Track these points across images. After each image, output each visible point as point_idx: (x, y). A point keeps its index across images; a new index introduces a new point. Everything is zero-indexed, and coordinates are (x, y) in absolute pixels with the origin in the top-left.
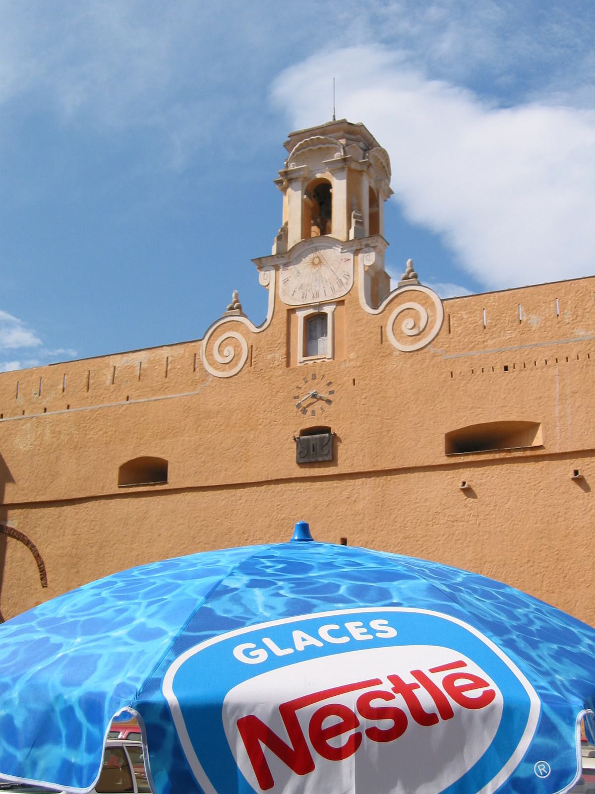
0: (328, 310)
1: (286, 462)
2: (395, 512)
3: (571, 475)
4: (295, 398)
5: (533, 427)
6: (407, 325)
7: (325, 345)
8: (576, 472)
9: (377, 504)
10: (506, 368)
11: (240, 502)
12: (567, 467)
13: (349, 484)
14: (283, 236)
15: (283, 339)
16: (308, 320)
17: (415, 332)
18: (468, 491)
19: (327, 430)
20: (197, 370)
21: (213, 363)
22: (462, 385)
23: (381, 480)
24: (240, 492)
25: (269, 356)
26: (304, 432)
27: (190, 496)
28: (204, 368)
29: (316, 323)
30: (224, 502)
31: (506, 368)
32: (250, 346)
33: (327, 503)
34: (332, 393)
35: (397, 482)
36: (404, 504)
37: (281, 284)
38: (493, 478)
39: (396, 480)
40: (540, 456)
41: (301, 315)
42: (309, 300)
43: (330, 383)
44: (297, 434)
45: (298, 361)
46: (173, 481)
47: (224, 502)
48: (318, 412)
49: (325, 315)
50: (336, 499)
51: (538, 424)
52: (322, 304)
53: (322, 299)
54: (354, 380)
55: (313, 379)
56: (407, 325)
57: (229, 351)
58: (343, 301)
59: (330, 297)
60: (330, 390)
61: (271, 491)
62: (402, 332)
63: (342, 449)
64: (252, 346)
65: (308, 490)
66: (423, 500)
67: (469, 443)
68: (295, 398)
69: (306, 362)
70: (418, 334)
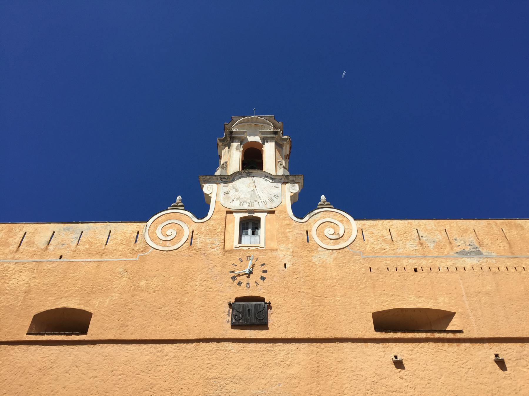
2: (331, 379)
3: (493, 357)
4: (231, 272)
5: (449, 316)
8: (497, 356)
9: (312, 369)
10: (416, 270)
11: (167, 358)
13: (283, 348)
15: (220, 229)
18: (399, 364)
19: (262, 300)
22: (381, 277)
23: (314, 346)
24: (168, 347)
26: (237, 300)
27: (110, 348)
29: (250, 224)
30: (148, 357)
31: (416, 270)
32: (191, 231)
33: (261, 365)
34: (265, 271)
35: (330, 350)
36: (340, 371)
38: (422, 355)
39: (329, 349)
41: (238, 216)
42: (246, 206)
43: (264, 264)
44: (232, 301)
45: (234, 246)
46: (92, 333)
47: (148, 357)
50: (270, 362)
51: (454, 313)
52: (254, 212)
53: (256, 207)
54: (285, 265)
55: (247, 260)
58: (273, 212)
59: (262, 207)
60: (264, 269)
61: (202, 349)
63: (273, 318)
64: (193, 231)
65: (240, 352)
66: (358, 369)
67: (393, 323)
68: (231, 272)
69: (240, 248)
70: (339, 239)
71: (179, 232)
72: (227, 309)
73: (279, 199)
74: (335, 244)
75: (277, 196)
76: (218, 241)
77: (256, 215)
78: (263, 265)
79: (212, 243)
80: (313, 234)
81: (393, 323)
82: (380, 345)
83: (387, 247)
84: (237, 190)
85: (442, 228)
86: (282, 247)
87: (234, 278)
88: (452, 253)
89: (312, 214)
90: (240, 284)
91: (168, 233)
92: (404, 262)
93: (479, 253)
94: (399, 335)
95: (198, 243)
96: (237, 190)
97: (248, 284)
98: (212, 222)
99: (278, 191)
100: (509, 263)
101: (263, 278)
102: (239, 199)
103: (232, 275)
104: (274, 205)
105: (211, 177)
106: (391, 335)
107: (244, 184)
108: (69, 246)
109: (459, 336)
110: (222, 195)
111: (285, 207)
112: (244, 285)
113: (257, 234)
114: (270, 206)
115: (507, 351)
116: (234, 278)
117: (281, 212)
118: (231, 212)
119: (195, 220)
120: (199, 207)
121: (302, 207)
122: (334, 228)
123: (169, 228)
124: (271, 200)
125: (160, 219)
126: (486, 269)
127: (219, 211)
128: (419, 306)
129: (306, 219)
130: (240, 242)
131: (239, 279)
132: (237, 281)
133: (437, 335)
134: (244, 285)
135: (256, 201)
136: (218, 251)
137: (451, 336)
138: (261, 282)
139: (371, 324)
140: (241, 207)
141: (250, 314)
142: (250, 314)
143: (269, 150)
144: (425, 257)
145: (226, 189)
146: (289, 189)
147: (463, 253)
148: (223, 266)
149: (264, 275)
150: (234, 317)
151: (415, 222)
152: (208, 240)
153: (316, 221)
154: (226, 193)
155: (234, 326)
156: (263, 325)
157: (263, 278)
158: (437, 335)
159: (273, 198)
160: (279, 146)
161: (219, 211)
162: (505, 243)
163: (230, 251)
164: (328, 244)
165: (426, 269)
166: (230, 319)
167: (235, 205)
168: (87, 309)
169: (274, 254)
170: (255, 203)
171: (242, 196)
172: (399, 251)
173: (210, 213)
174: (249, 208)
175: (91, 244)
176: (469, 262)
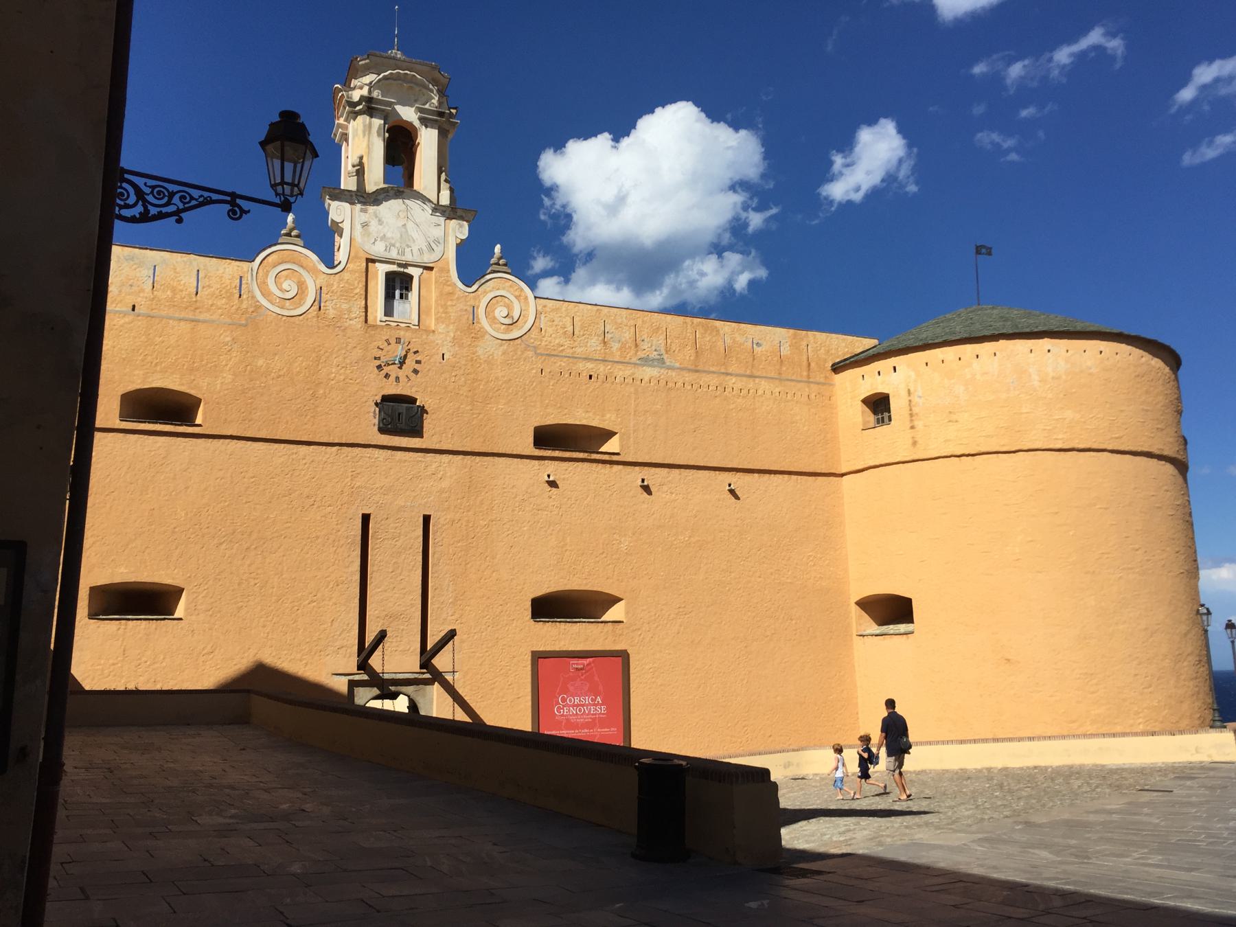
0: (414, 272)
1: (367, 426)
6: (500, 312)
7: (406, 309)
10: (590, 377)
15: (360, 289)
16: (391, 279)
17: (508, 321)
19: (414, 400)
20: (244, 296)
21: (266, 294)
25: (345, 306)
26: (386, 399)
28: (253, 297)
29: (398, 283)
31: (590, 377)
34: (418, 362)
37: (358, 227)
38: (574, 474)
40: (612, 461)
41: (381, 270)
42: (393, 254)
52: (406, 266)
53: (408, 257)
56: (500, 312)
57: (290, 287)
58: (431, 269)
59: (416, 258)
62: (495, 318)
63: (428, 423)
67: (552, 439)
71: (302, 286)
72: (373, 408)
73: (441, 247)
74: (506, 332)
75: (437, 241)
76: (358, 311)
77: (410, 270)
79: (350, 311)
80: (481, 311)
81: (552, 439)
82: (536, 462)
83: (567, 343)
84: (380, 222)
85: (632, 323)
86: (441, 328)
87: (379, 367)
88: (634, 360)
89: (483, 280)
90: (387, 376)
91: (285, 286)
94: (557, 454)
95: (330, 310)
96: (380, 222)
97: (397, 379)
98: (346, 275)
99: (438, 233)
101: (416, 372)
102: (384, 238)
103: (378, 362)
106: (548, 453)
108: (142, 290)
109: (615, 458)
110: (358, 227)
112: (392, 378)
113: (407, 298)
114: (427, 259)
116: (379, 367)
118: (374, 261)
119: (322, 267)
121: (472, 265)
123: (287, 277)
125: (270, 259)
126: (663, 383)
128: (584, 422)
129: (475, 287)
130: (389, 311)
131: (386, 369)
133: (594, 456)
134: (392, 378)
135: (408, 246)
136: (358, 323)
137: (606, 457)
138: (413, 376)
139: (531, 439)
141: (401, 416)
142: (401, 416)
143: (428, 142)
145: (364, 217)
146: (454, 230)
147: (646, 361)
148: (366, 349)
149: (417, 367)
150: (381, 420)
152: (345, 306)
153: (485, 292)
154: (365, 225)
155: (382, 430)
156: (417, 432)
157: (416, 372)
158: (594, 456)
159: (434, 246)
161: (356, 257)
163: (375, 327)
164: (497, 330)
165: (602, 377)
166: (376, 421)
167: (378, 250)
168: (193, 392)
169: (431, 337)
170: (407, 250)
171: (389, 235)
172: (579, 350)
174: (399, 257)
175: (174, 290)
176: (649, 372)
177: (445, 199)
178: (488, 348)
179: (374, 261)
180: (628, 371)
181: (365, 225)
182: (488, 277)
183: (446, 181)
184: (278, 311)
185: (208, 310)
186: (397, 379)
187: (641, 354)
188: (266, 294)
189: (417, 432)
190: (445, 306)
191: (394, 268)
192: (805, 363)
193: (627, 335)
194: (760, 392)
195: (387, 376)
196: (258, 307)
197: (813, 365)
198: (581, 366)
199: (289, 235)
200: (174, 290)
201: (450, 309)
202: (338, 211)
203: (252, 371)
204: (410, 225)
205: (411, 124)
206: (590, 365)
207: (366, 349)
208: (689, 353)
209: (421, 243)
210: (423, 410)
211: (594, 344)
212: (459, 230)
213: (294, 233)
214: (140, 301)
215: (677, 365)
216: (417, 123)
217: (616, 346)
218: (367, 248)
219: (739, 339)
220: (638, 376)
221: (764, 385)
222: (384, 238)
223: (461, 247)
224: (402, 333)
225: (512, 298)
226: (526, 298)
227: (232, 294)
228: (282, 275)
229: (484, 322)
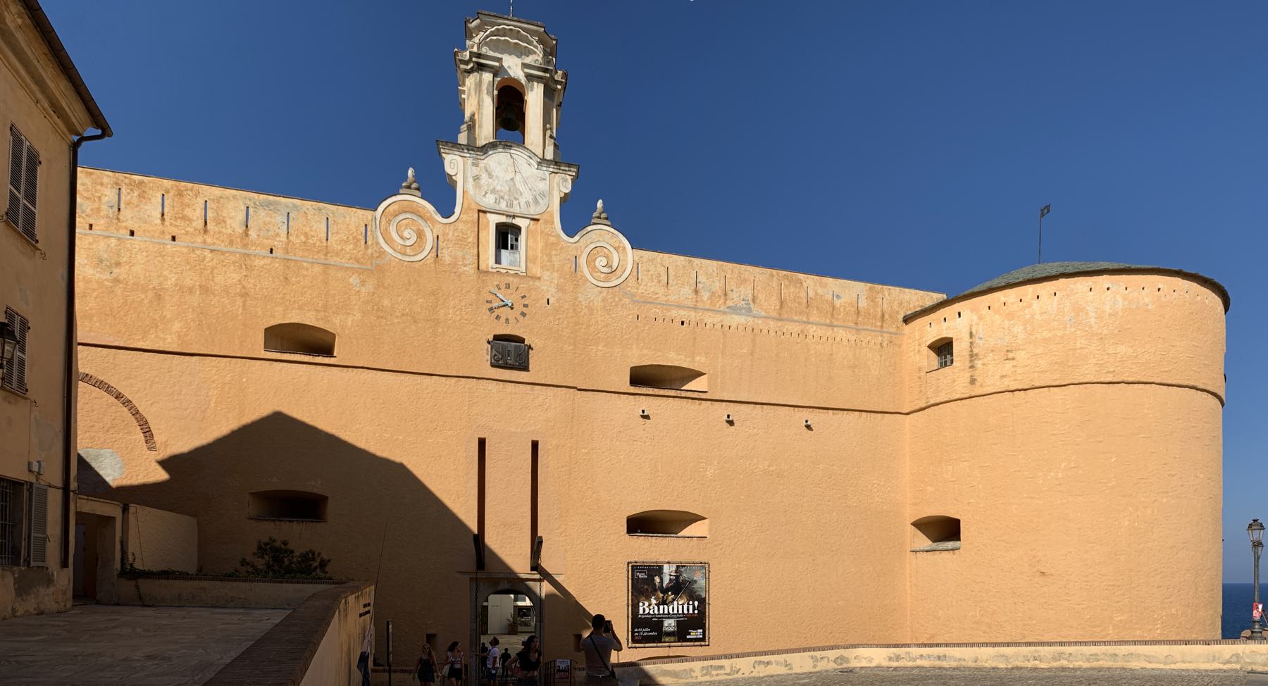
6: (601, 262)
12: (722, 411)
14: (471, 128)
15: (472, 239)
17: (606, 270)
19: (522, 340)
21: (388, 241)
26: (497, 338)
28: (378, 243)
34: (525, 306)
40: (699, 397)
41: (494, 220)
42: (503, 206)
48: (512, 320)
49: (517, 229)
56: (601, 262)
59: (525, 211)
71: (420, 235)
75: (542, 195)
76: (471, 259)
77: (517, 221)
78: (524, 297)
79: (464, 258)
80: (582, 261)
83: (661, 291)
86: (546, 275)
87: (491, 309)
88: (723, 308)
89: (584, 231)
91: (406, 234)
92: (674, 313)
93: (750, 310)
94: (650, 391)
95: (446, 256)
97: (507, 320)
98: (460, 226)
99: (543, 186)
100: (772, 324)
101: (523, 314)
102: (494, 191)
103: (489, 306)
104: (539, 209)
105: (456, 145)
107: (499, 161)
108: (277, 235)
110: (471, 180)
111: (552, 216)
112: (503, 320)
114: (533, 211)
115: (737, 412)
116: (491, 309)
117: (546, 222)
118: (485, 212)
119: (438, 218)
120: (442, 194)
121: (575, 216)
122: (607, 257)
123: (407, 226)
124: (536, 201)
125: (391, 208)
126: (749, 330)
127: (469, 208)
128: (676, 364)
129: (577, 238)
130: (498, 261)
131: (497, 312)
132: (494, 315)
133: (684, 394)
134: (503, 320)
136: (470, 269)
140: (497, 207)
141: (510, 353)
143: (534, 99)
144: (695, 308)
145: (475, 171)
147: (735, 310)
148: (479, 293)
149: (525, 310)
151: (697, 261)
152: (459, 254)
154: (476, 178)
155: (492, 365)
156: (525, 368)
157: (523, 314)
160: (549, 93)
161: (469, 208)
162: (778, 303)
163: (487, 272)
167: (488, 201)
169: (537, 283)
170: (515, 202)
171: (498, 188)
172: (672, 298)
173: (458, 209)
175: (306, 235)
176: (736, 320)
177: (549, 155)
178: (591, 295)
179: (485, 212)
180: (717, 318)
181: (476, 178)
182: (589, 228)
183: (551, 137)
184: (400, 257)
185: (337, 254)
186: (507, 320)
187: (730, 303)
188: (388, 241)
189: (525, 368)
190: (550, 255)
191: (503, 219)
192: (879, 314)
193: (717, 286)
194: (838, 339)
195: (498, 317)
196: (382, 253)
197: (886, 316)
198: (674, 313)
199: (409, 187)
200: (306, 235)
201: (554, 258)
202: (454, 163)
203: (378, 310)
204: (518, 178)
205: (518, 82)
206: (682, 312)
207: (479, 293)
208: (774, 302)
209: (527, 196)
210: (530, 347)
211: (687, 291)
212: (563, 183)
213: (414, 186)
214: (278, 244)
215: (763, 314)
216: (523, 80)
217: (705, 295)
218: (478, 200)
219: (820, 291)
220: (726, 323)
221: (841, 333)
222: (494, 191)
223: (564, 200)
224: (511, 279)
225: (612, 249)
226: (624, 249)
227: (358, 241)
228: (403, 220)
229: (586, 271)
